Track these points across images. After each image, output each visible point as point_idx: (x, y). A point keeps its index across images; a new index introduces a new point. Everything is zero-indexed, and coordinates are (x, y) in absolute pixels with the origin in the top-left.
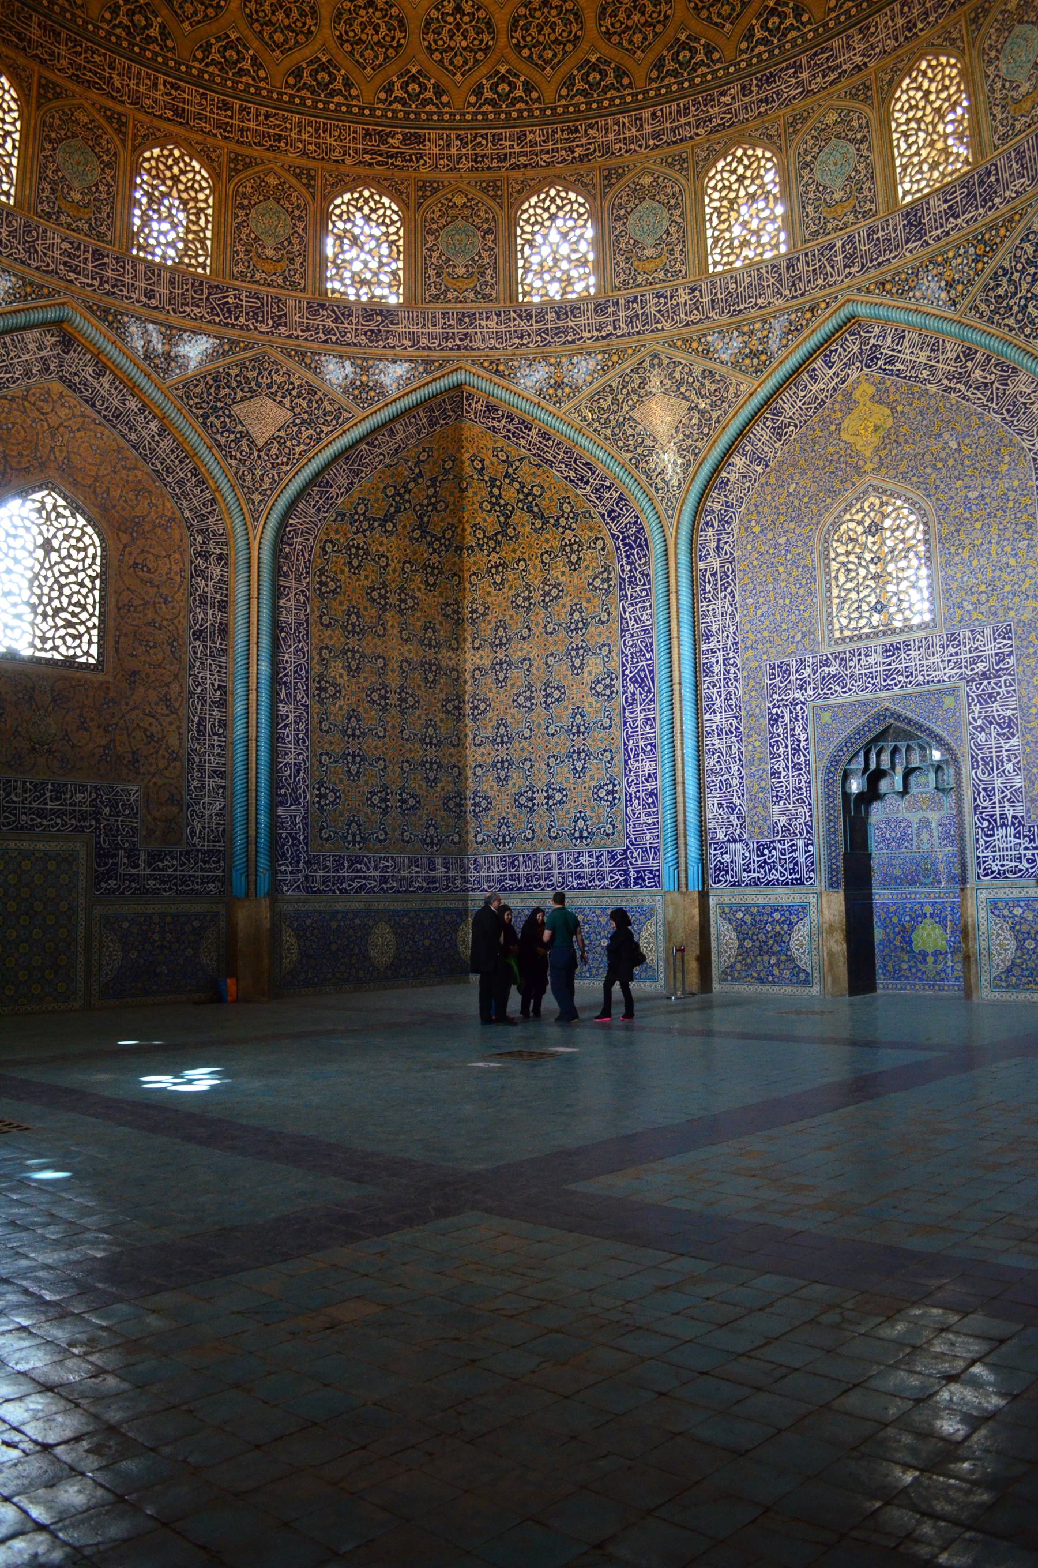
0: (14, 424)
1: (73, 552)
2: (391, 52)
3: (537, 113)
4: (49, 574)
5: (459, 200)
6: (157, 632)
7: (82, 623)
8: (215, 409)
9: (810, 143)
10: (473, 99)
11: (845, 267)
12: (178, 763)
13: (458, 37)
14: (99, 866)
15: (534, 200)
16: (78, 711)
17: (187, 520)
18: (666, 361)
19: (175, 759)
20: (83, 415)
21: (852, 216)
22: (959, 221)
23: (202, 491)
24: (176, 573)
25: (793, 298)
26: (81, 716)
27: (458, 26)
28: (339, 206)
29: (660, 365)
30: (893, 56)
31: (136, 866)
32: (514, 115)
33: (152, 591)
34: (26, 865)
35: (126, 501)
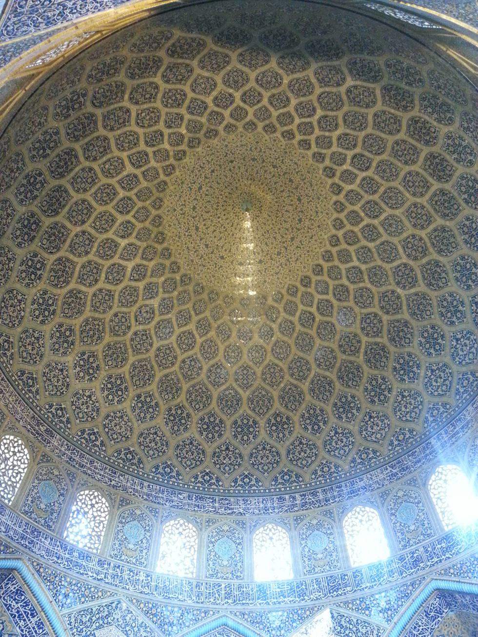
2: (58, 393)
3: (102, 456)
5: (56, 472)
9: (215, 534)
10: (79, 434)
11: (225, 598)
13: (84, 407)
15: (87, 492)
18: (124, 608)
21: (230, 575)
22: (286, 599)
25: (197, 602)
27: (87, 402)
28: (7, 439)
29: (121, 609)
30: (257, 516)
32: (93, 451)
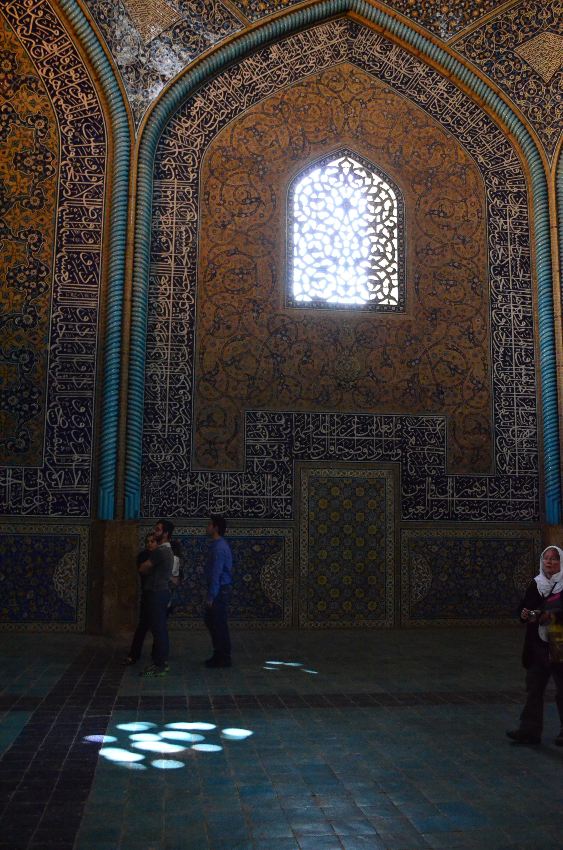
0: (310, 105)
1: (371, 208)
4: (349, 229)
6: (455, 271)
7: (382, 269)
8: (498, 55)
12: (484, 394)
14: (406, 491)
16: (381, 350)
17: (481, 165)
19: (480, 389)
20: (373, 87)
23: (495, 137)
24: (473, 215)
26: (384, 353)
31: (445, 492)
33: (450, 234)
34: (335, 492)
35: (419, 156)
